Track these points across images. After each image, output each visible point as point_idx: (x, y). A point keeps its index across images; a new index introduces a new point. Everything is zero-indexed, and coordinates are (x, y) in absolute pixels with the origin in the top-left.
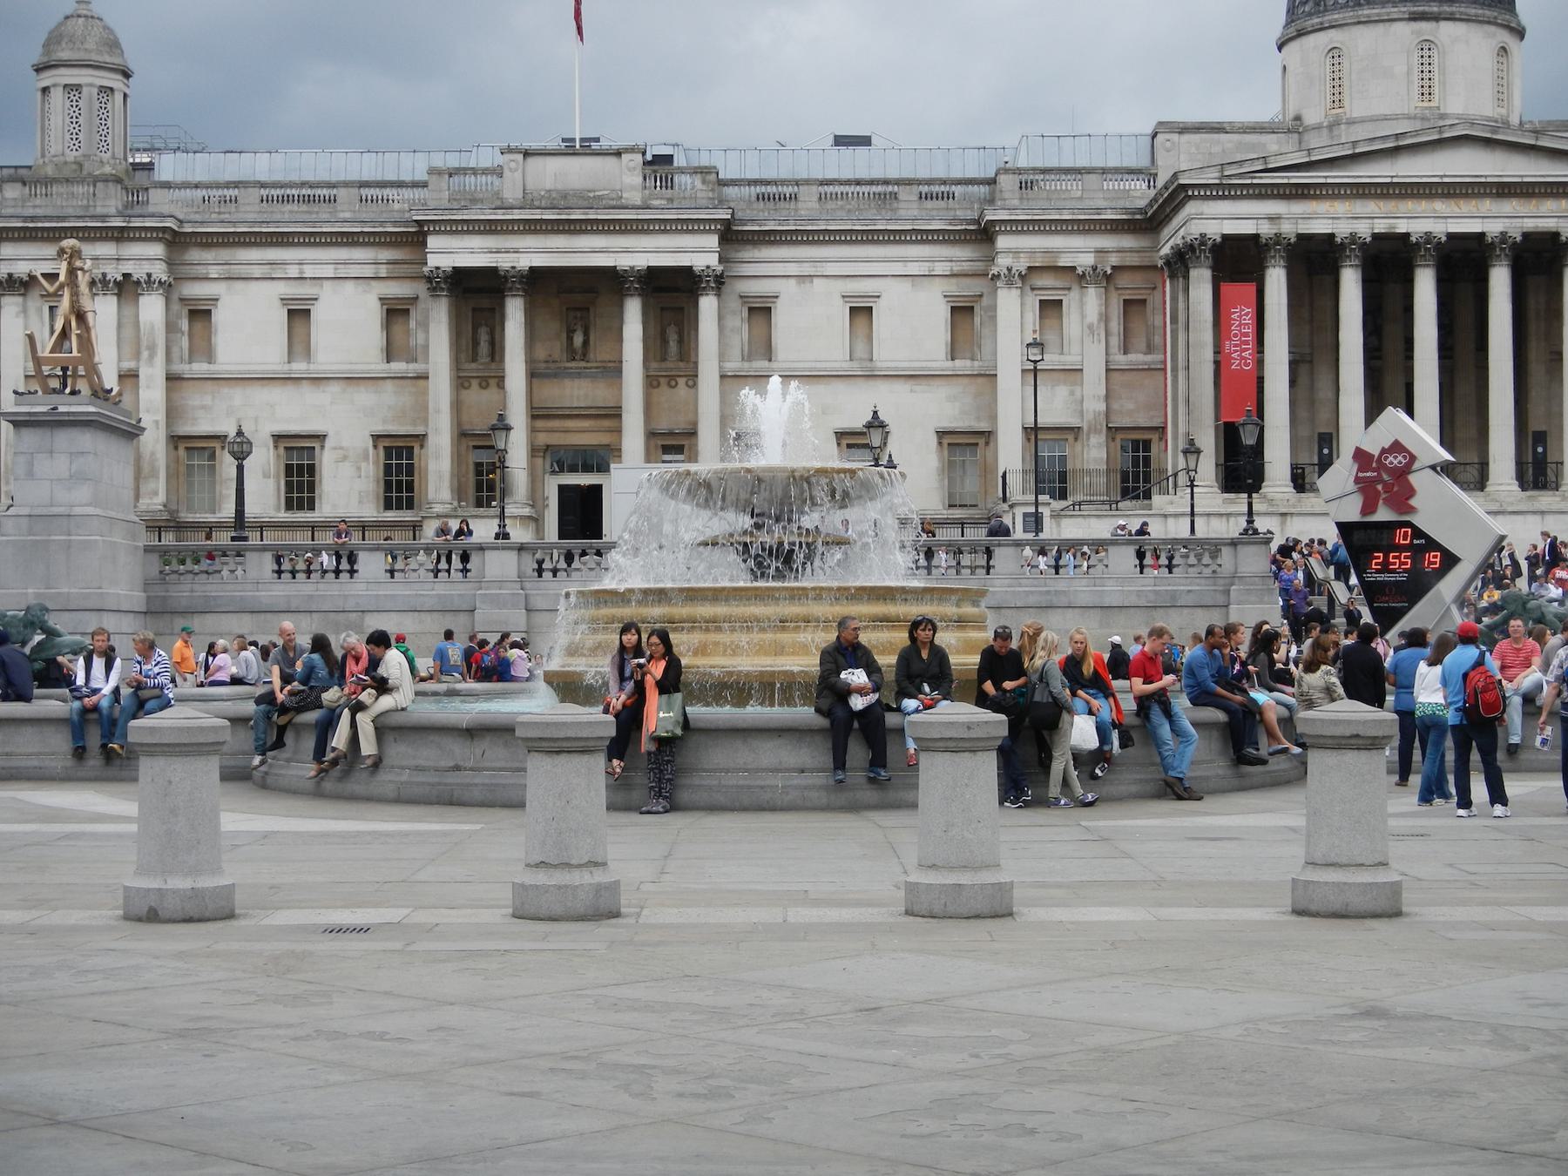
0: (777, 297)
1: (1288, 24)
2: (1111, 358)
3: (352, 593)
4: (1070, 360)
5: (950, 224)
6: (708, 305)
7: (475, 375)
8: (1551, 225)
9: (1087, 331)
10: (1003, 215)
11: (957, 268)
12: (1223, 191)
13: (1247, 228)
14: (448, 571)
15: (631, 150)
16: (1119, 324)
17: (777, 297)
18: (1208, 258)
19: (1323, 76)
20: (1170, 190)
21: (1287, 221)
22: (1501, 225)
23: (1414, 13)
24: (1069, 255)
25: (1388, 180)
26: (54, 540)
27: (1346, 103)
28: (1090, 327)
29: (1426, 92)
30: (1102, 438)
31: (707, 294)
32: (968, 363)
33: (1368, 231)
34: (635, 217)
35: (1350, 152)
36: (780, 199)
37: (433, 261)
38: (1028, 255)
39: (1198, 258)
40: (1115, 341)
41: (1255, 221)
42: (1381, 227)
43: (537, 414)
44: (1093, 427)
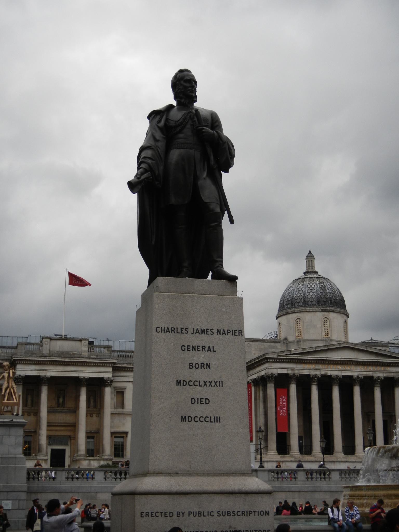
0: (126, 388)
3: (93, 486)
6: (108, 391)
7: (26, 411)
8: (371, 374)
12: (279, 360)
13: (285, 372)
14: (38, 478)
15: (85, 339)
17: (126, 388)
19: (295, 326)
21: (296, 370)
23: (323, 309)
25: (326, 359)
26: (11, 467)
27: (302, 335)
29: (326, 333)
31: (108, 387)
33: (319, 374)
34: (86, 361)
35: (314, 350)
36: (127, 357)
37: (18, 373)
41: (287, 370)
42: (323, 373)
43: (49, 425)
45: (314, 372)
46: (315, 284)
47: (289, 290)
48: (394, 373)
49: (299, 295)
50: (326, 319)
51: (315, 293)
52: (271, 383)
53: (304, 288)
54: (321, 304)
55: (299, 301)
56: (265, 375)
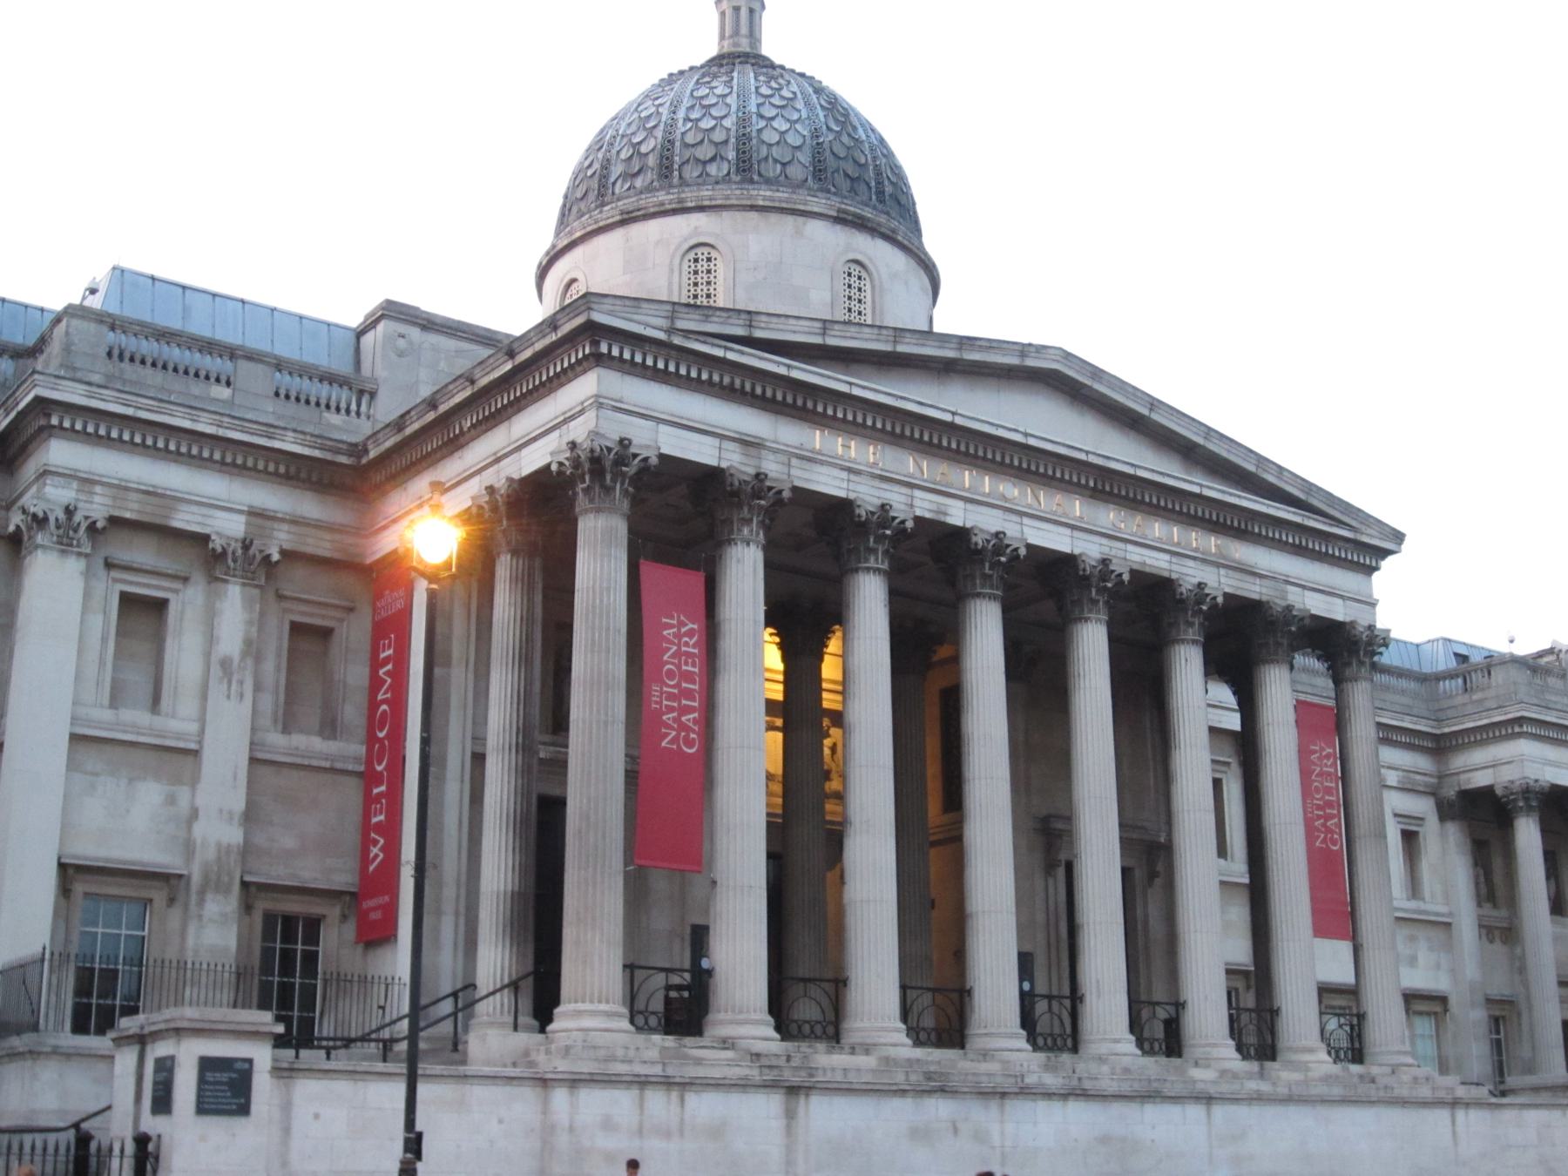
1: (557, 234)
4: (177, 723)
8: (1165, 565)
9: (216, 671)
10: (73, 394)
13: (702, 452)
16: (278, 669)
20: (560, 334)
21: (771, 457)
24: (194, 509)
25: (947, 417)
28: (225, 664)
30: (232, 903)
35: (888, 348)
38: (107, 491)
39: (608, 490)
41: (716, 442)
42: (925, 505)
45: (877, 493)
46: (794, 88)
47: (639, 109)
48: (1266, 582)
49: (707, 124)
50: (858, 268)
51: (798, 126)
52: (611, 510)
53: (738, 96)
54: (834, 186)
55: (709, 156)
56: (561, 458)
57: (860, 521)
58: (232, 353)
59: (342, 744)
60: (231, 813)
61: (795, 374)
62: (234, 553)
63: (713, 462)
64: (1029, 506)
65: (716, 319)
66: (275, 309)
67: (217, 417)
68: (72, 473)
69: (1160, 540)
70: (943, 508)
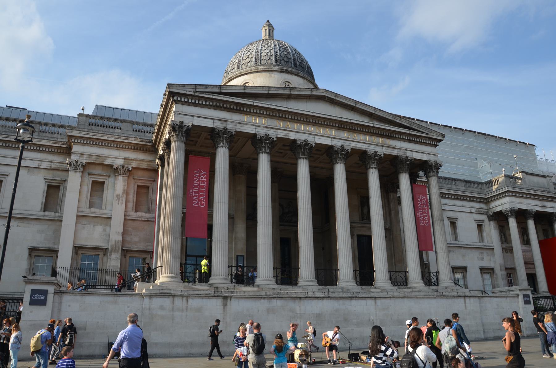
2: (128, 213)
4: (105, 212)
5: (53, 143)
8: (363, 147)
9: (115, 198)
10: (76, 133)
11: (53, 166)
13: (208, 124)
18: (183, 136)
21: (230, 124)
22: (341, 143)
23: (283, 69)
24: (110, 159)
25: (286, 109)
28: (118, 196)
30: (119, 255)
32: (53, 214)
40: (130, 205)
41: (212, 121)
42: (281, 134)
44: (114, 248)
45: (265, 131)
48: (398, 150)
50: (288, 83)
57: (258, 139)
58: (121, 121)
59: (151, 214)
60: (119, 232)
61: (235, 101)
62: (120, 169)
63: (212, 126)
64: (317, 133)
65: (210, 88)
66: (138, 111)
67: (114, 136)
68: (78, 153)
69: (362, 140)
70: (287, 135)
